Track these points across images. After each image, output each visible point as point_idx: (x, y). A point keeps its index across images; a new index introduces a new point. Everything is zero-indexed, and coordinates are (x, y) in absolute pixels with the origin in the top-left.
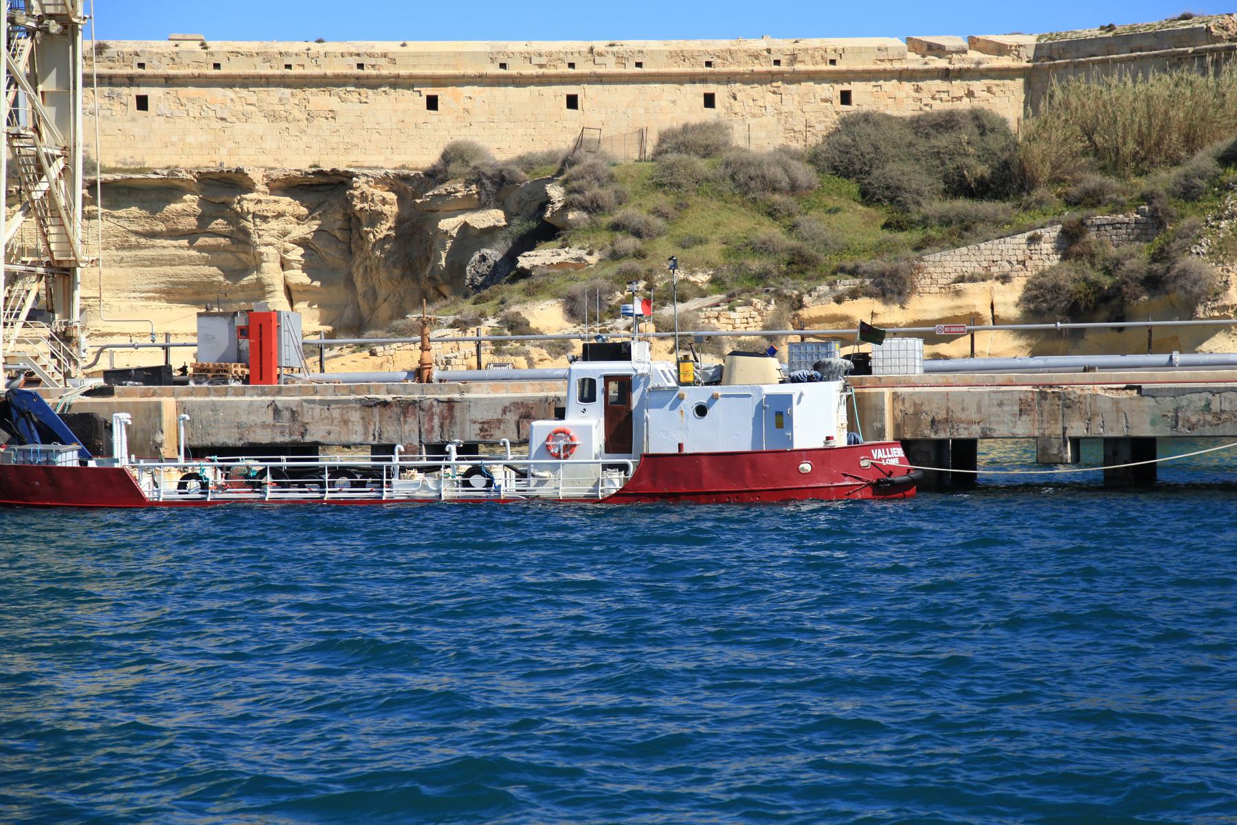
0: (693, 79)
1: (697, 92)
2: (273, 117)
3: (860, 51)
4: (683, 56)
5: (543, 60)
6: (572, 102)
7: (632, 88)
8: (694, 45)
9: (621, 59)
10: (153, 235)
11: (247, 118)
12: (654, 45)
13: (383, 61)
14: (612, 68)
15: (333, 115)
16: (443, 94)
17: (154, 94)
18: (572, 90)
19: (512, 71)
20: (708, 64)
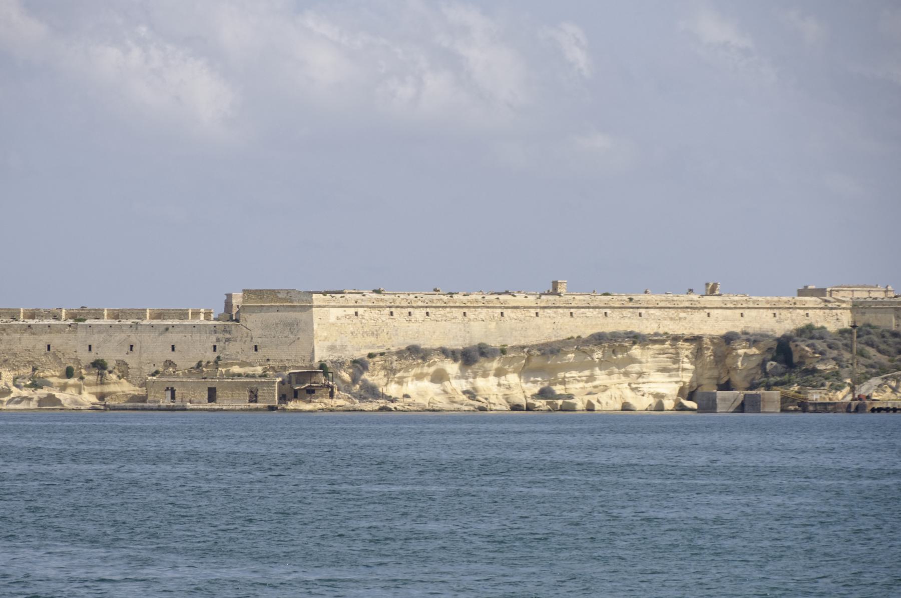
0: (771, 308)
1: (770, 312)
2: (671, 319)
3: (810, 301)
4: (767, 302)
5: (735, 303)
6: (742, 315)
7: (756, 310)
8: (769, 298)
9: (754, 302)
10: (660, 354)
11: (665, 319)
12: (760, 299)
13: (697, 303)
14: (751, 305)
15: (685, 318)
16: (712, 312)
17: (643, 311)
18: (741, 311)
19: (728, 306)
20: (775, 304)
